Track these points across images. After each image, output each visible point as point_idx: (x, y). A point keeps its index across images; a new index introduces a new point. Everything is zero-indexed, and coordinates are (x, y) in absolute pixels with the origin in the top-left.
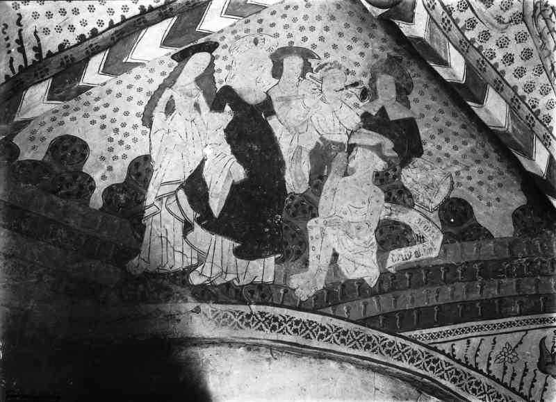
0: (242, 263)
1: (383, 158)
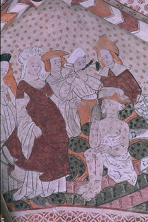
0: (46, 184)
1: (119, 101)
